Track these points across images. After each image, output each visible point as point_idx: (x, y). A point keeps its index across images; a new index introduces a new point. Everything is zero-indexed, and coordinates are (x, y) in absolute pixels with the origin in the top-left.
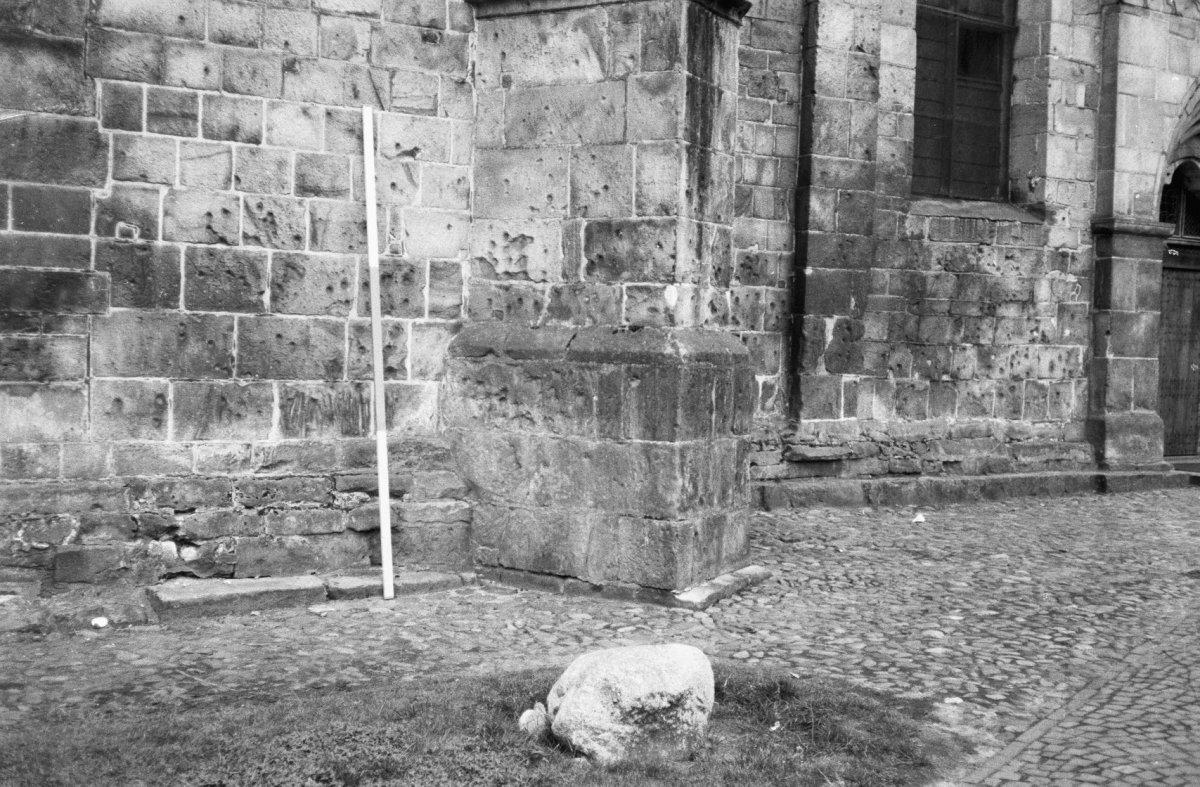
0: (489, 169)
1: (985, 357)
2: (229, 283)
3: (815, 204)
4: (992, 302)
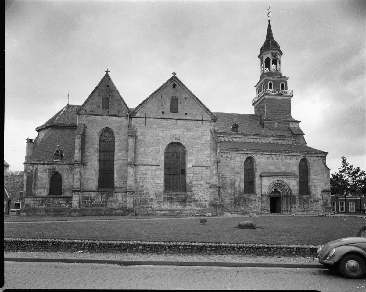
0: (210, 195)
1: (251, 205)
2: (198, 201)
3: (236, 195)
4: (252, 201)
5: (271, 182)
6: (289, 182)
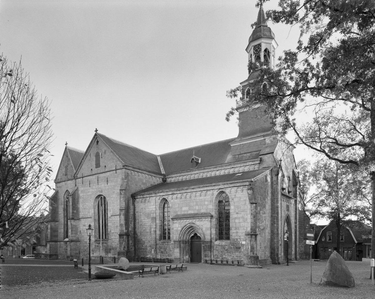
5: (183, 225)
6: (202, 224)
